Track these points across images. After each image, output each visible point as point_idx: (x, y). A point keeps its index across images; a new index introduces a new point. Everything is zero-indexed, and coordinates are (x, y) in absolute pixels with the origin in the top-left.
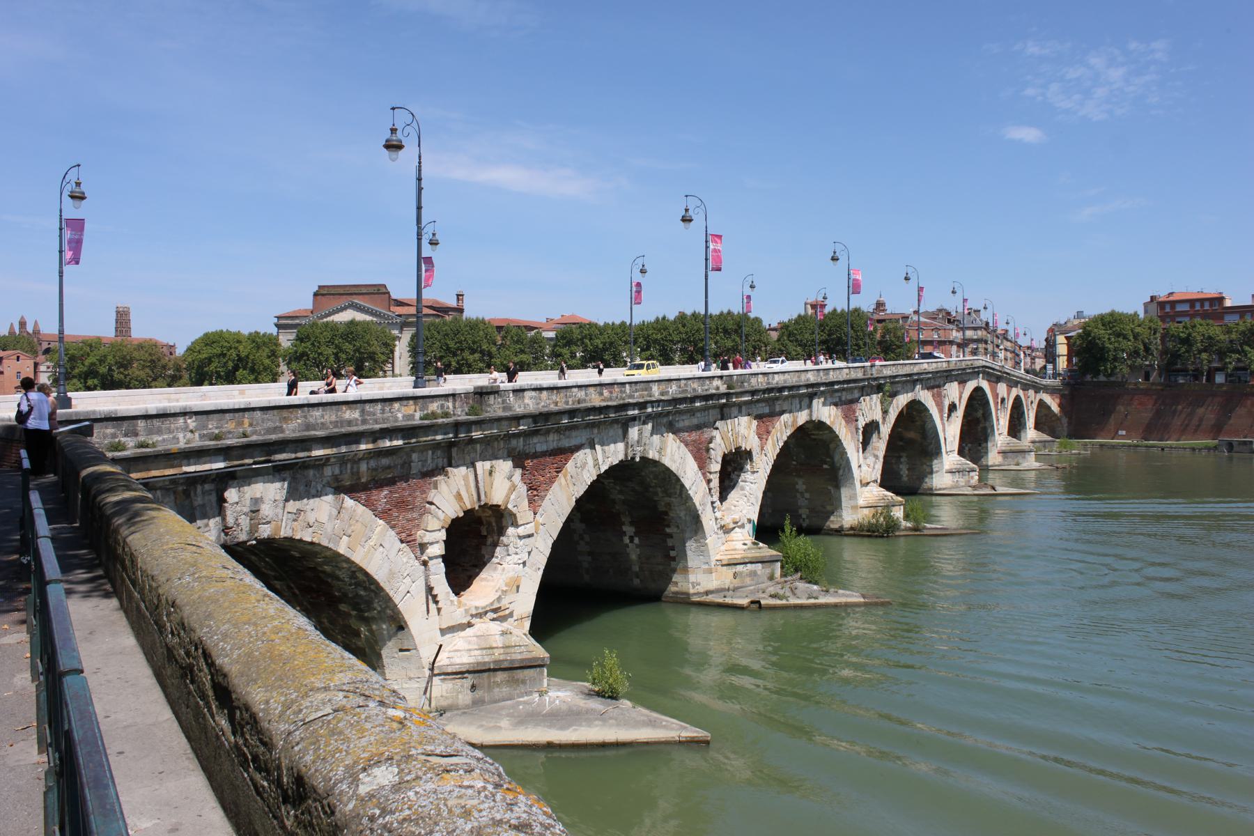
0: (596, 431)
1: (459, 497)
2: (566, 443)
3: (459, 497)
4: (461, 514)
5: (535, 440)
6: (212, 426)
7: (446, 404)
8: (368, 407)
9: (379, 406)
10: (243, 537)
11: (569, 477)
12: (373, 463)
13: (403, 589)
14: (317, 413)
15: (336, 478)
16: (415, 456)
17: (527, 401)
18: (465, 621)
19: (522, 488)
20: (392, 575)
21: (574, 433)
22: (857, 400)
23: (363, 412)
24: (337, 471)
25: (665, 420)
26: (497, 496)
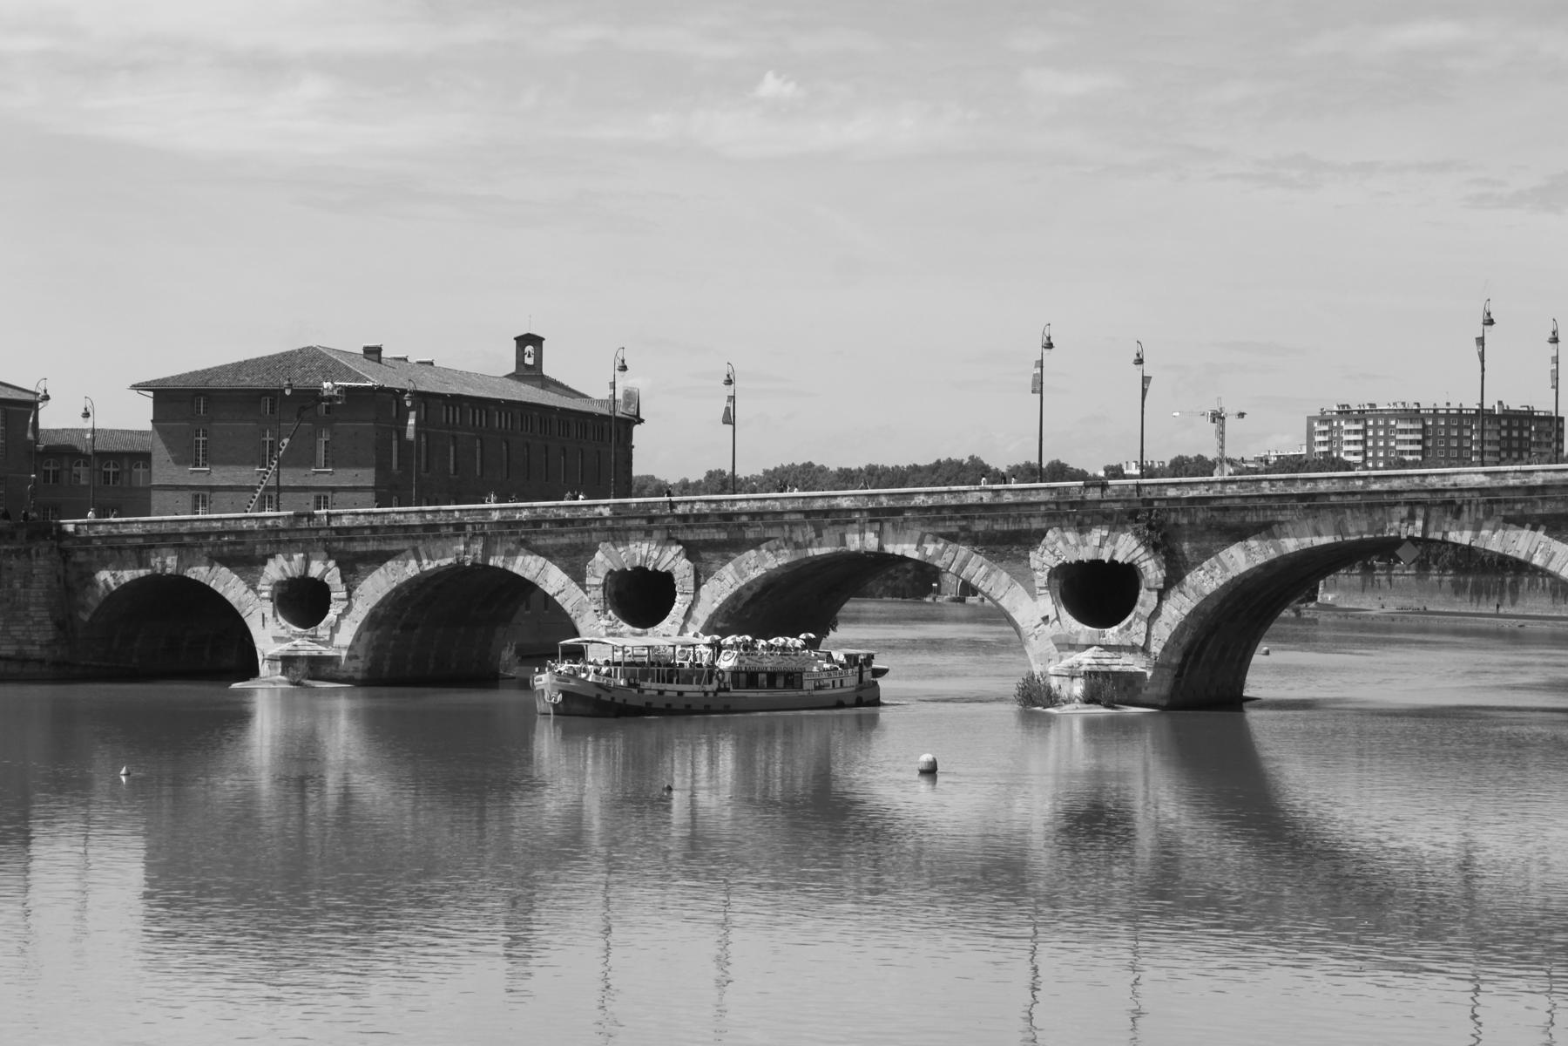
0: (420, 542)
1: (283, 570)
2: (386, 547)
3: (283, 570)
4: (285, 579)
5: (355, 544)
6: (148, 527)
7: (277, 521)
8: (227, 522)
9: (233, 522)
10: (159, 572)
11: (389, 569)
12: (231, 548)
13: (248, 611)
14: (198, 524)
15: (209, 553)
16: (258, 547)
17: (344, 521)
18: (287, 636)
19: (336, 571)
20: (240, 603)
21: (395, 542)
22: (1042, 534)
23: (223, 524)
24: (210, 549)
25: (514, 538)
26: (316, 569)
